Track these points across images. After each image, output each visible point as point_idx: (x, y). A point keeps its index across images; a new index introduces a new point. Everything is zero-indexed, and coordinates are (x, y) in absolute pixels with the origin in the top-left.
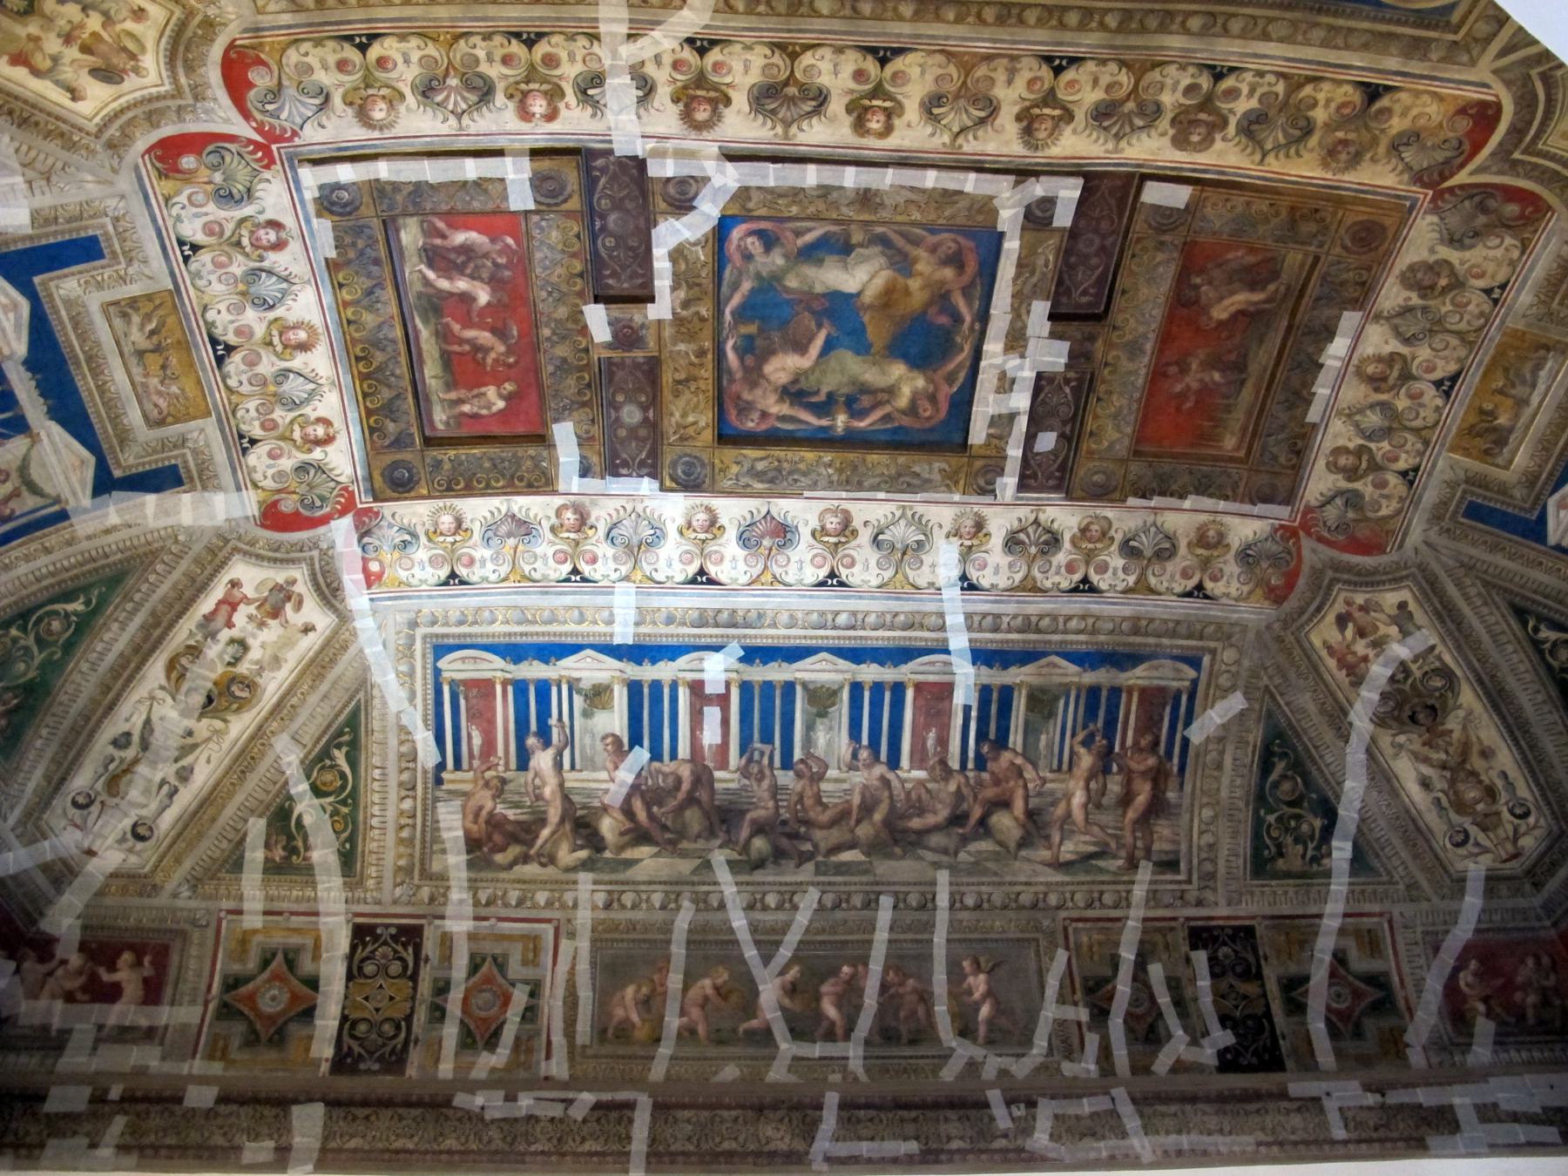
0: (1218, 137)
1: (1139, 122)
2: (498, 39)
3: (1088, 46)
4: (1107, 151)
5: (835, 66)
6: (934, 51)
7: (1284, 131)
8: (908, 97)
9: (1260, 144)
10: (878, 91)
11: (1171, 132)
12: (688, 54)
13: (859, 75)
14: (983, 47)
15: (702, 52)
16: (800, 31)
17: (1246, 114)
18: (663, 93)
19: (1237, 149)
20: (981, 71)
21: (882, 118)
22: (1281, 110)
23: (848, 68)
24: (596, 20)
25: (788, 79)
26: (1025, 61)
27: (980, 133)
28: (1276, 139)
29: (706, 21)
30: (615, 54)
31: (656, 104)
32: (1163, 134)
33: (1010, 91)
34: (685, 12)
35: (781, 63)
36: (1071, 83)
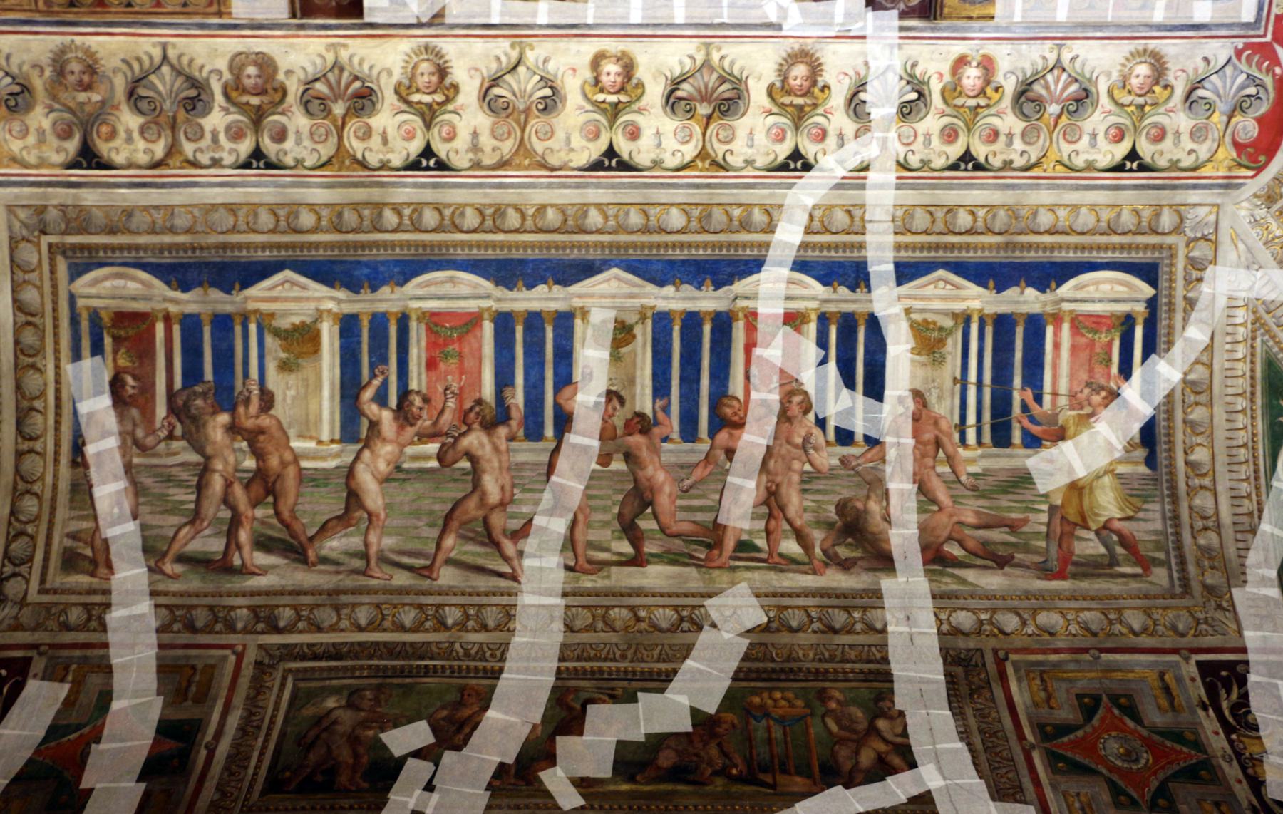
0: (227, 76)
1: (320, 87)
2: (996, 162)
3: (405, 185)
4: (345, 46)
5: (660, 144)
6: (560, 169)
7: (159, 93)
8: (581, 108)
9: (178, 72)
10: (614, 112)
11: (281, 76)
12: (809, 149)
13: (634, 134)
14: (512, 176)
15: (796, 155)
16: (697, 186)
17: (207, 111)
18: (837, 99)
19: (199, 62)
20: (508, 146)
21: (604, 79)
22: (174, 118)
23: (646, 140)
24: (898, 187)
25: (707, 124)
26: (467, 164)
27: (494, 66)
28: (162, 79)
29: (793, 191)
30: (884, 144)
31: (847, 81)
32: (289, 72)
33: (473, 123)
34: (810, 202)
35: (716, 145)
36: (410, 136)
